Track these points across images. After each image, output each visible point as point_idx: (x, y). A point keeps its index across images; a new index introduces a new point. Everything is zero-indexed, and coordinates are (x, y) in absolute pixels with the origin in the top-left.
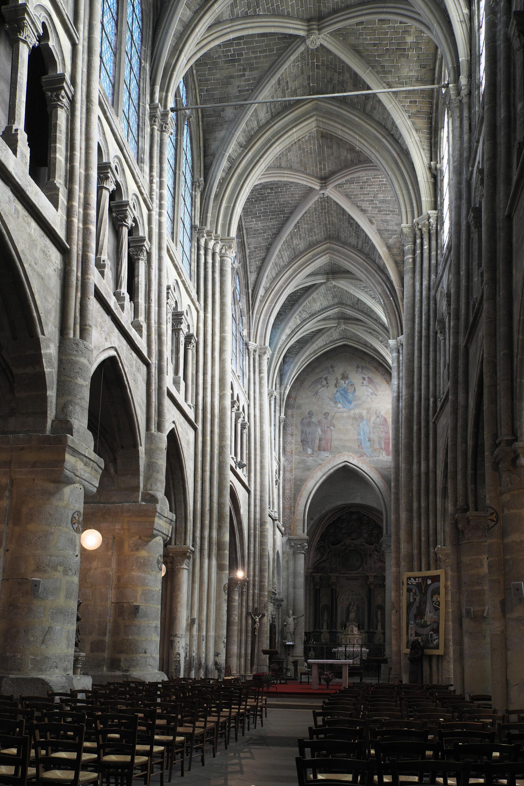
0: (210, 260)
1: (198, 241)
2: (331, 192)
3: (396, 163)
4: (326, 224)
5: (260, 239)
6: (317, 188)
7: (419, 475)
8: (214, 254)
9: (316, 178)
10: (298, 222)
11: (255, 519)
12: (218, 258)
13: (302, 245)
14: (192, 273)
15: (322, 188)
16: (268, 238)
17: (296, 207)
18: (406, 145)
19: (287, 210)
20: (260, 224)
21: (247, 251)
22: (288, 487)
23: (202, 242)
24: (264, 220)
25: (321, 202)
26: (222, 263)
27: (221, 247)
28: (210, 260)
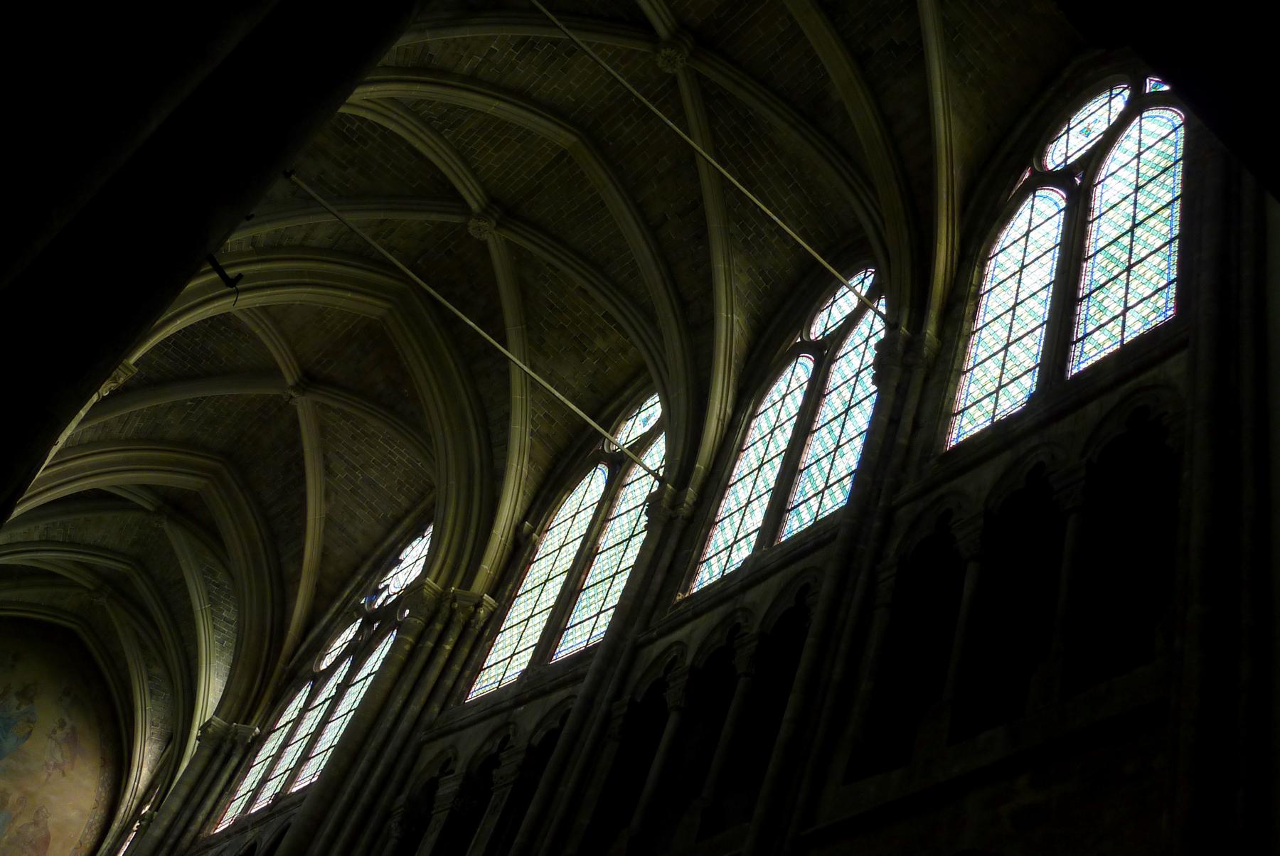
3: (470, 477)
6: (290, 381)
15: (296, 387)
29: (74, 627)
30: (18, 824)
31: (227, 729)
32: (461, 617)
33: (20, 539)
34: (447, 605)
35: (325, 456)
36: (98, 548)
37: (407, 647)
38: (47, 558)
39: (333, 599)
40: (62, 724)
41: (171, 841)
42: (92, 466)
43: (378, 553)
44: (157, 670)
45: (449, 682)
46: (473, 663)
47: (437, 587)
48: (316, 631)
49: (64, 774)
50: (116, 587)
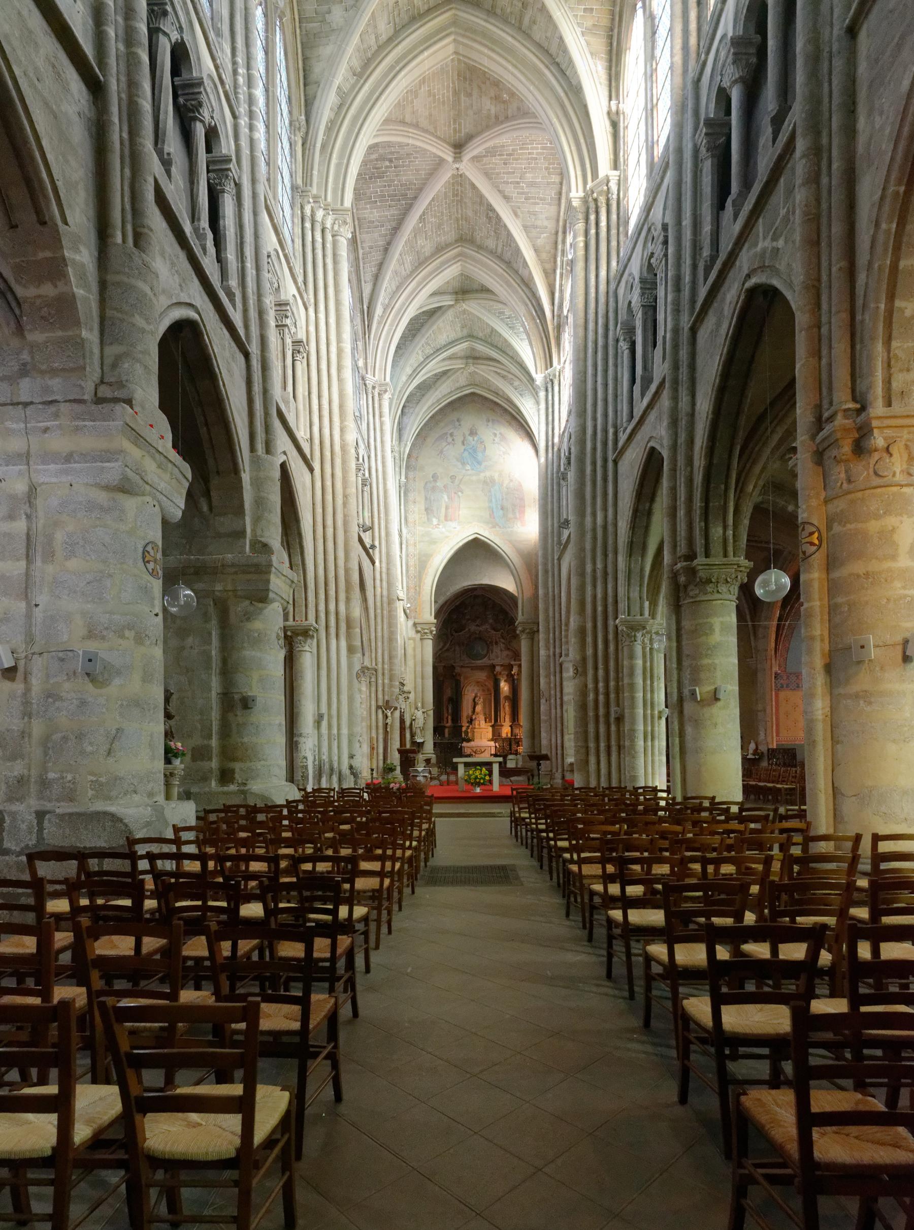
0: (319, 238)
2: (466, 167)
5: (376, 235)
6: (450, 159)
7: (594, 530)
8: (323, 231)
9: (448, 143)
12: (329, 238)
13: (428, 249)
14: (297, 254)
16: (386, 235)
17: (421, 190)
18: (578, 77)
19: (410, 194)
21: (361, 252)
22: (411, 563)
25: (453, 184)
26: (335, 244)
28: (319, 238)
29: (472, 390)
32: (602, 200)
34: (590, 199)
35: (499, 191)
36: (450, 343)
38: (434, 366)
39: (555, 271)
40: (495, 435)
41: (550, 443)
42: (407, 300)
43: (561, 223)
44: (517, 383)
47: (581, 194)
48: (557, 295)
50: (473, 357)
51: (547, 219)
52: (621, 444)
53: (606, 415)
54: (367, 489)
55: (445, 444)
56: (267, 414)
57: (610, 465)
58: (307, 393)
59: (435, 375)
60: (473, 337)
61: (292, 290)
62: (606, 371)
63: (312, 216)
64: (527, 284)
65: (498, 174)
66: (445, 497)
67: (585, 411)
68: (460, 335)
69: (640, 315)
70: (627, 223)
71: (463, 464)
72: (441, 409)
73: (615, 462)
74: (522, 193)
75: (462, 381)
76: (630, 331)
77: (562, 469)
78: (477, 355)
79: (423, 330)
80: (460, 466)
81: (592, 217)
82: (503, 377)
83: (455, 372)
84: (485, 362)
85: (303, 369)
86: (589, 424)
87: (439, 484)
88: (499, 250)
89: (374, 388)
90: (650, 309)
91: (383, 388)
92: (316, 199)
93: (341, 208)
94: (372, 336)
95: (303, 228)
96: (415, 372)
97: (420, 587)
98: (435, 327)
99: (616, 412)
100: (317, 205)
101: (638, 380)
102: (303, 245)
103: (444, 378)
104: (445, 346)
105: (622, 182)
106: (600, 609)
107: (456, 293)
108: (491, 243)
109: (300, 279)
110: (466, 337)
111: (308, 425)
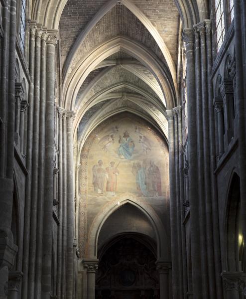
0: (39, 45)
1: (31, 30)
4: (119, 24)
5: (70, 32)
8: (42, 41)
10: (99, 22)
11: (63, 246)
12: (45, 44)
14: (26, 54)
16: (76, 32)
17: (98, 10)
20: (70, 21)
23: (34, 31)
24: (73, 18)
26: (48, 48)
27: (47, 36)
28: (39, 45)
30: (147, 169)
31: (173, 112)
32: (201, 33)
33: (91, 97)
34: (195, 32)
36: (112, 85)
37: (191, 54)
38: (102, 97)
40: (141, 137)
41: (176, 151)
45: (209, 55)
46: (213, 44)
47: (190, 28)
48: (179, 67)
49: (150, 150)
50: (125, 91)
51: (172, 28)
52: (218, 165)
53: (208, 147)
54: (56, 175)
55: (107, 142)
56: (9, 155)
57: (213, 176)
58: (26, 130)
59: (103, 101)
60: (127, 82)
61: (23, 75)
62: (207, 122)
63: (36, 34)
64: (160, 59)
65: (143, 5)
66: (107, 176)
67: (196, 143)
68: (118, 81)
69: (225, 97)
70: (216, 46)
71: (119, 155)
72: (105, 121)
73: (216, 175)
74: (157, 15)
75: (119, 105)
76: (220, 103)
77: (185, 167)
78: (130, 91)
79: (95, 79)
80: (117, 156)
81: (197, 40)
82: (146, 103)
83: (115, 100)
84: (135, 95)
85: (25, 116)
86: (199, 151)
87: (103, 167)
88: (143, 41)
89: (64, 114)
90: (230, 94)
91: (70, 114)
92: (39, 26)
93: (53, 30)
94: (64, 85)
95: (30, 41)
96: (90, 101)
97: (87, 236)
98: (103, 77)
99: (214, 146)
100: (39, 29)
101: (226, 132)
102: (30, 50)
103: (108, 103)
104: (109, 86)
105: (214, 26)
106: (210, 265)
107: (117, 59)
108: (139, 37)
109: (27, 67)
110: (122, 82)
111: (26, 148)
